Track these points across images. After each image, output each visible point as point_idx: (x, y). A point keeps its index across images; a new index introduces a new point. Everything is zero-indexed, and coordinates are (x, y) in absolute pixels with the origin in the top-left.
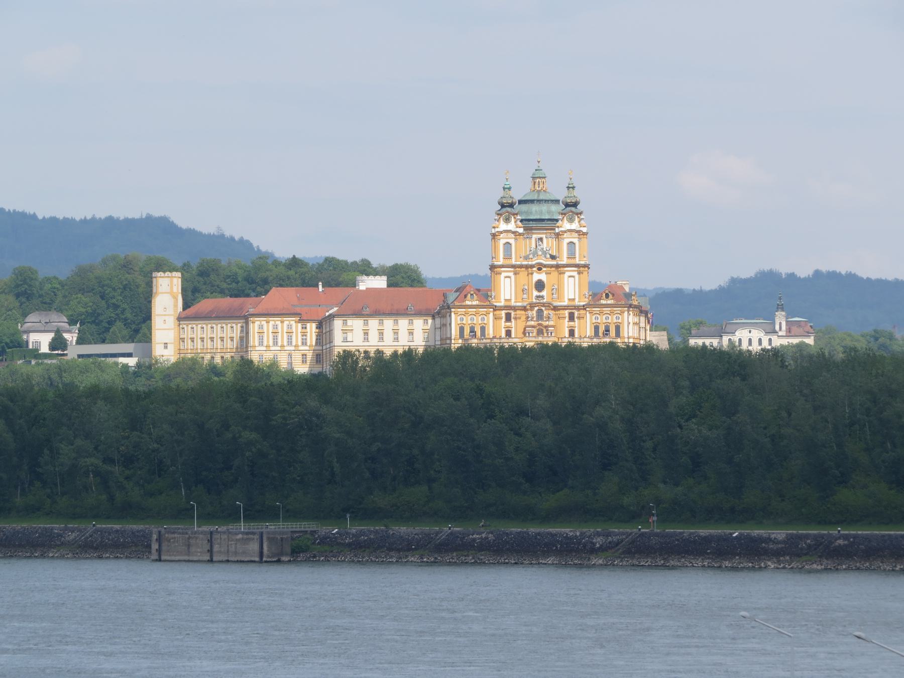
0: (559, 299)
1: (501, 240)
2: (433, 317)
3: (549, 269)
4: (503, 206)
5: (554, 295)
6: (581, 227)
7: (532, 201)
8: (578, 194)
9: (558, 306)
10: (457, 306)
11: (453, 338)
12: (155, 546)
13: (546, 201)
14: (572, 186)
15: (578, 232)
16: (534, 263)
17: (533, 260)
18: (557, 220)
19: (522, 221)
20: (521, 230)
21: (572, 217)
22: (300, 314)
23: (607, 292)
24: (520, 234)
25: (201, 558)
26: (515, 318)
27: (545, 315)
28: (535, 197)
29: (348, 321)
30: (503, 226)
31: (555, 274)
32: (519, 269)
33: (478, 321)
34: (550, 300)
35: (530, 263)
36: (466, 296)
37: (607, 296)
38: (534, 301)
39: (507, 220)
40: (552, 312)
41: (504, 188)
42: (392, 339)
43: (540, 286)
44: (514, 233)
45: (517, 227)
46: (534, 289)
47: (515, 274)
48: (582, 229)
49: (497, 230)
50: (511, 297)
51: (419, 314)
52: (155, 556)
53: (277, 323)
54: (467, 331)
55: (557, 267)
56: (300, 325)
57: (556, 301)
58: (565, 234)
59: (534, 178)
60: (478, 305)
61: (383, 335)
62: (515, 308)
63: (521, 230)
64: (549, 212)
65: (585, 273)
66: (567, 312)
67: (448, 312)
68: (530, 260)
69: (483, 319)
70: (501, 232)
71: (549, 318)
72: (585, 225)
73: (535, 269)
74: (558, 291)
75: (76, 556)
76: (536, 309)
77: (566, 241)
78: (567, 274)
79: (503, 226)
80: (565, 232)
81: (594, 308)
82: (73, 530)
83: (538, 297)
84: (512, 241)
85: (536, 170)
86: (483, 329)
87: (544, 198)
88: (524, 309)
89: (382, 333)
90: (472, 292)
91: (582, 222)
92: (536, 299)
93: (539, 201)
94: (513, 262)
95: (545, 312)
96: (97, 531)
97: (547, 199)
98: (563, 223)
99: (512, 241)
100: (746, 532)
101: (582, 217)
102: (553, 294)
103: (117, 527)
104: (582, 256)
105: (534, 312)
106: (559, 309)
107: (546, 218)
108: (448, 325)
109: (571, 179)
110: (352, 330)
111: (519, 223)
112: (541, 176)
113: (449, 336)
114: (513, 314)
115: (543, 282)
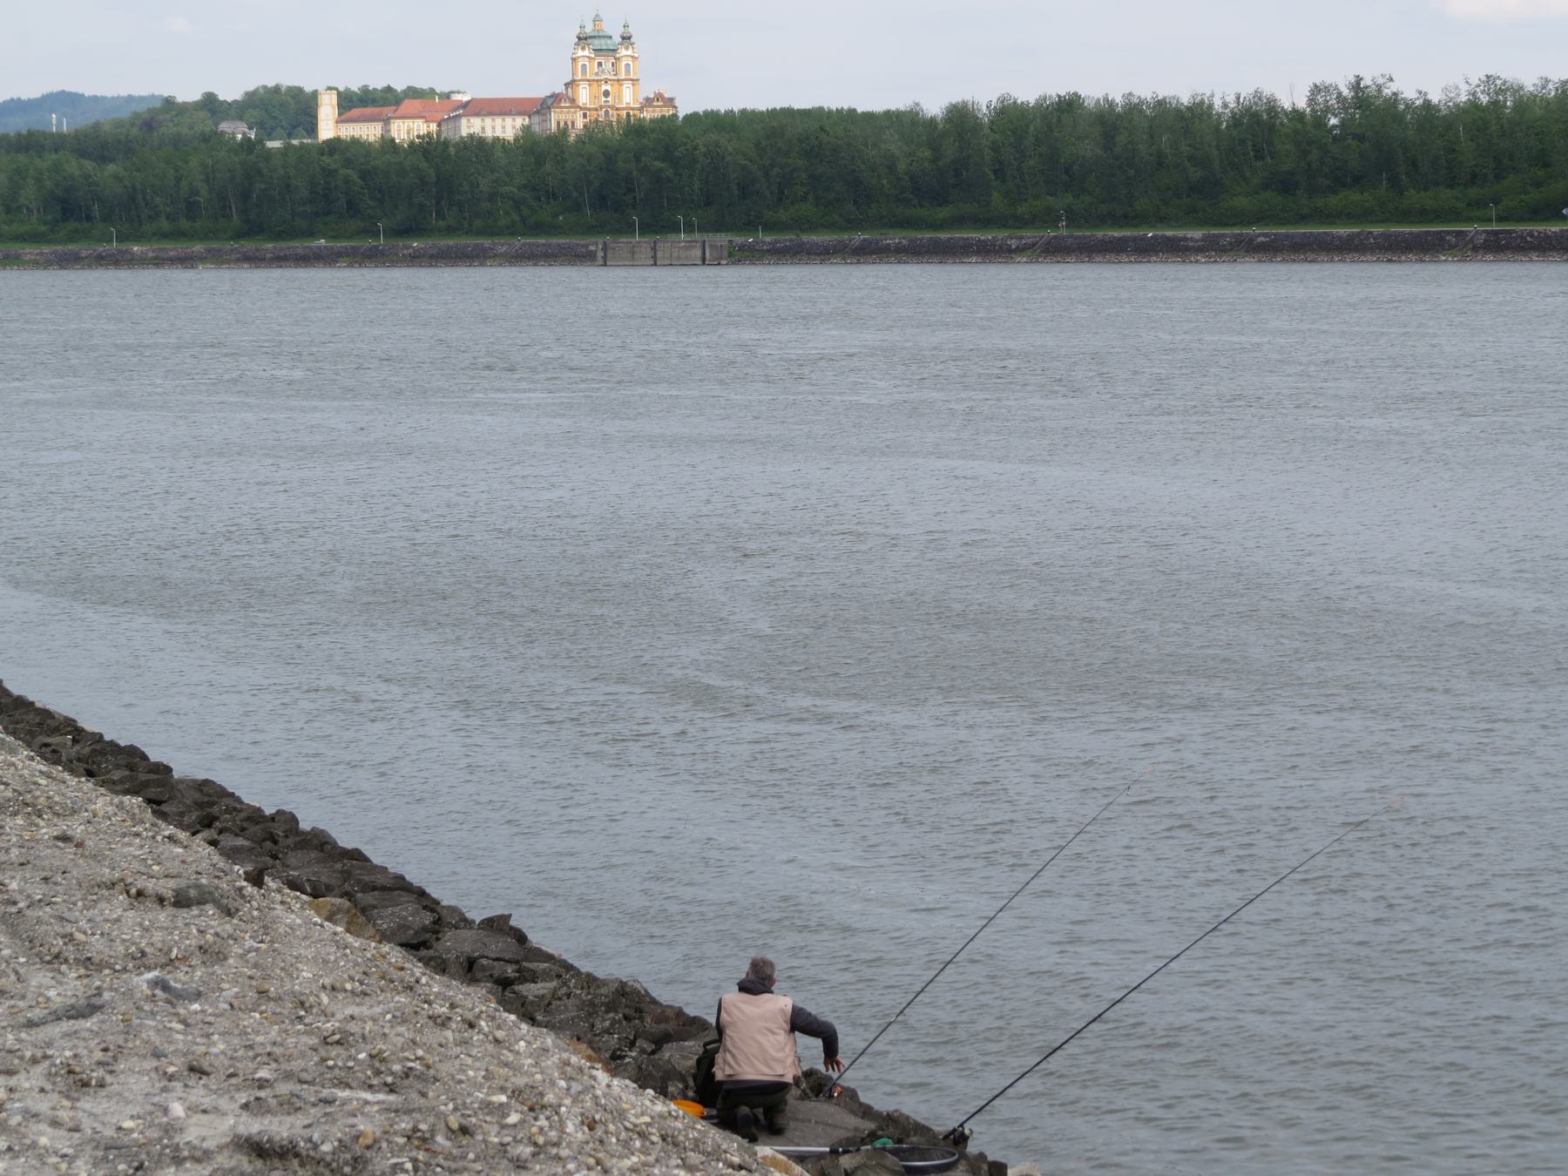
2: (530, 117)
4: (579, 39)
7: (594, 37)
12: (600, 254)
13: (604, 37)
20: (593, 56)
30: (580, 53)
31: (616, 86)
33: (569, 117)
39: (583, 49)
40: (615, 112)
43: (606, 94)
44: (589, 57)
47: (590, 85)
51: (520, 114)
52: (600, 261)
54: (562, 124)
55: (618, 80)
62: (589, 109)
63: (593, 56)
64: (607, 45)
66: (625, 112)
74: (620, 97)
75: (512, 264)
82: (502, 245)
84: (587, 64)
86: (573, 123)
88: (596, 110)
94: (588, 77)
96: (524, 245)
99: (587, 64)
100: (1159, 233)
103: (544, 241)
104: (635, 73)
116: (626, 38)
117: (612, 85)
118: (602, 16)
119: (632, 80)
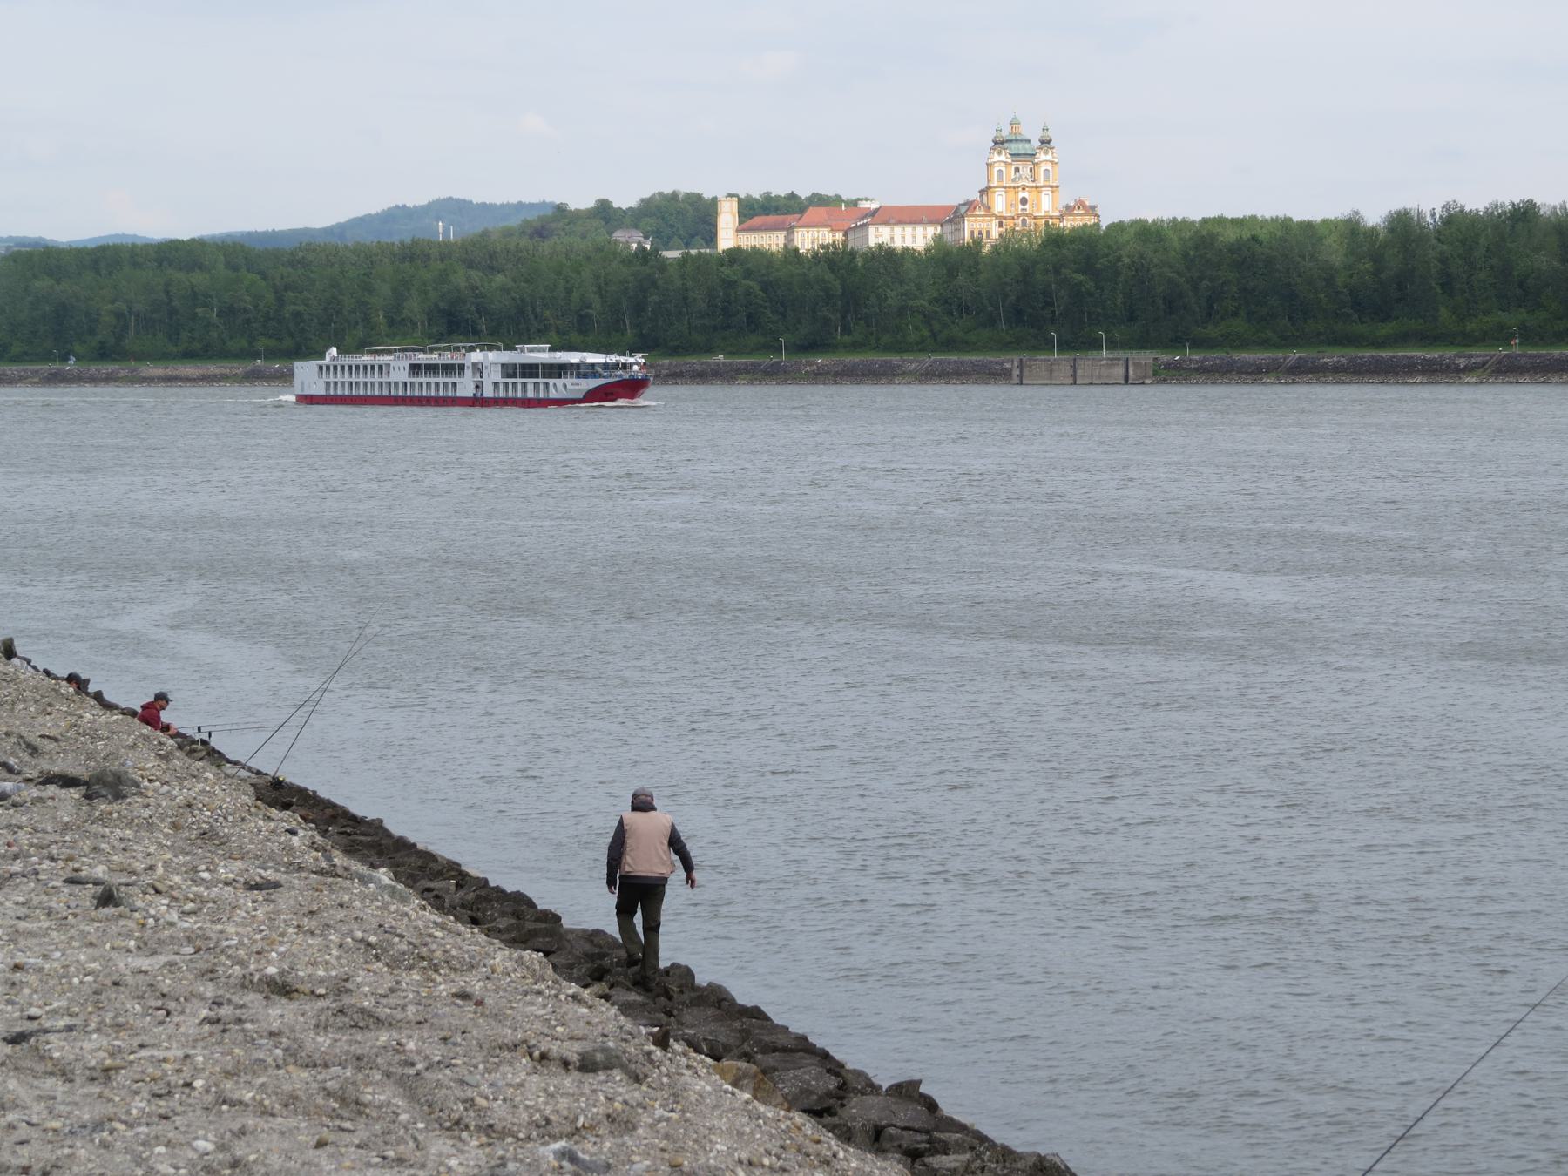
2: (942, 226)
4: (996, 143)
8: (1051, 134)
12: (1016, 372)
13: (1021, 141)
15: (1052, 162)
20: (1010, 161)
25: (1064, 382)
30: (996, 158)
36: (975, 208)
39: (999, 153)
40: (1033, 221)
43: (1024, 201)
44: (1005, 162)
51: (931, 222)
52: (1017, 380)
54: (976, 234)
55: (1037, 187)
62: (1005, 218)
63: (1010, 161)
64: (1024, 149)
66: (1043, 221)
74: (1038, 205)
75: (921, 382)
77: (1043, 169)
78: (1043, 193)
82: (912, 362)
84: (1004, 169)
86: (988, 232)
88: (1013, 218)
93: (1017, 141)
99: (1004, 169)
103: (956, 358)
104: (1054, 180)
116: (1045, 142)
118: (1020, 119)
119: (1051, 187)
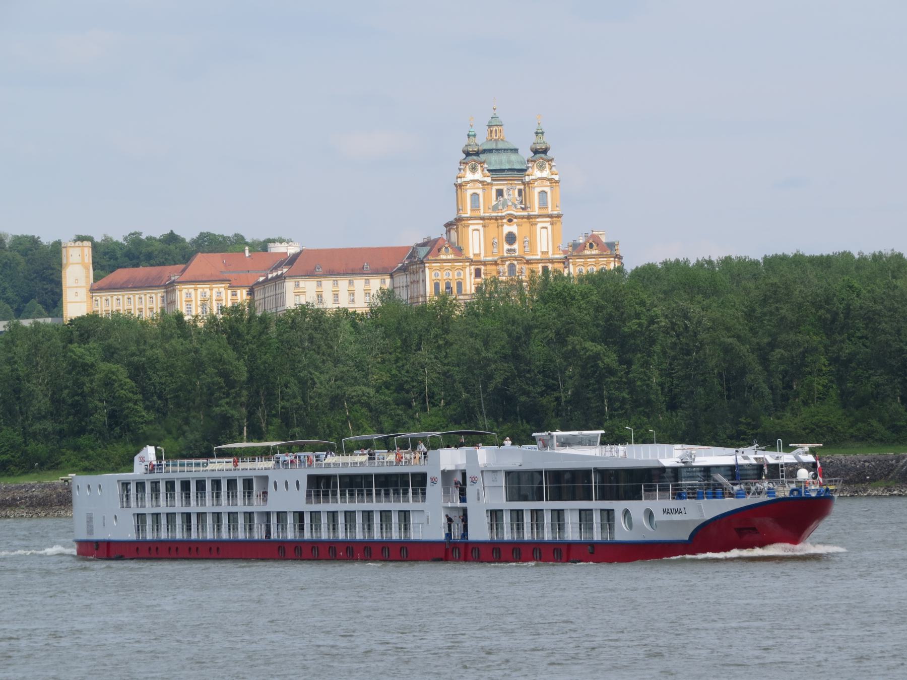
0: (531, 252)
1: (468, 190)
2: (392, 276)
3: (520, 220)
4: (468, 154)
5: (526, 248)
6: (552, 174)
7: (490, 151)
9: (530, 260)
10: (432, 260)
11: (428, 294)
13: (505, 150)
14: (541, 131)
15: (550, 180)
16: (504, 214)
17: (503, 211)
18: (525, 170)
19: (489, 171)
20: (489, 180)
21: (543, 164)
22: (229, 281)
23: (591, 241)
24: (488, 184)
26: (486, 274)
27: (517, 270)
28: (493, 146)
29: (301, 282)
30: (469, 176)
31: (526, 225)
32: (489, 221)
33: (453, 276)
34: (522, 254)
35: (500, 214)
36: (439, 250)
37: (591, 246)
38: (505, 255)
40: (525, 267)
41: (469, 136)
42: (348, 301)
43: (511, 238)
44: (482, 182)
45: (484, 177)
46: (505, 243)
47: (484, 226)
48: (554, 177)
49: (463, 180)
50: (480, 252)
51: (376, 272)
53: (206, 290)
54: (442, 287)
55: (529, 217)
56: (229, 292)
57: (527, 254)
58: (536, 183)
59: (490, 126)
60: (454, 260)
61: (353, 296)
62: (485, 263)
63: (489, 180)
64: (509, 162)
65: (558, 224)
67: (422, 268)
68: (500, 211)
69: (459, 274)
70: (468, 182)
71: (522, 272)
72: (556, 172)
73: (505, 221)
76: (508, 263)
77: (537, 190)
78: (539, 225)
79: (469, 176)
80: (536, 180)
81: (589, 258)
83: (509, 250)
84: (480, 192)
85: (492, 118)
86: (459, 285)
87: (503, 148)
88: (495, 263)
89: (353, 294)
90: (447, 246)
91: (554, 169)
92: (507, 253)
94: (482, 214)
95: (517, 266)
97: (506, 148)
98: (533, 170)
99: (480, 192)
101: (553, 164)
102: (525, 247)
104: (555, 206)
105: (506, 267)
106: (531, 263)
107: (507, 168)
108: (421, 282)
109: (539, 124)
110: (305, 292)
111: (487, 172)
112: (498, 124)
113: (422, 293)
114: (483, 268)
115: (514, 235)
117: (518, 225)
119: (551, 216)
